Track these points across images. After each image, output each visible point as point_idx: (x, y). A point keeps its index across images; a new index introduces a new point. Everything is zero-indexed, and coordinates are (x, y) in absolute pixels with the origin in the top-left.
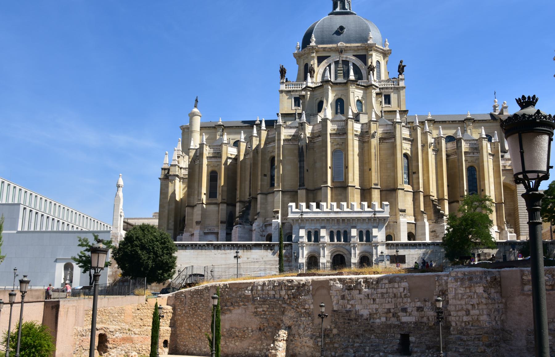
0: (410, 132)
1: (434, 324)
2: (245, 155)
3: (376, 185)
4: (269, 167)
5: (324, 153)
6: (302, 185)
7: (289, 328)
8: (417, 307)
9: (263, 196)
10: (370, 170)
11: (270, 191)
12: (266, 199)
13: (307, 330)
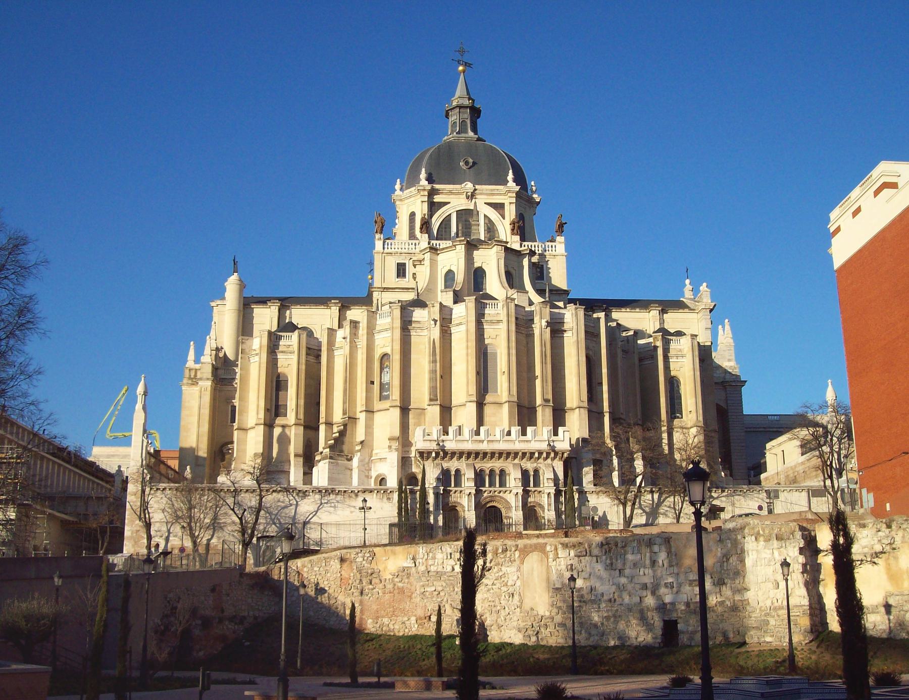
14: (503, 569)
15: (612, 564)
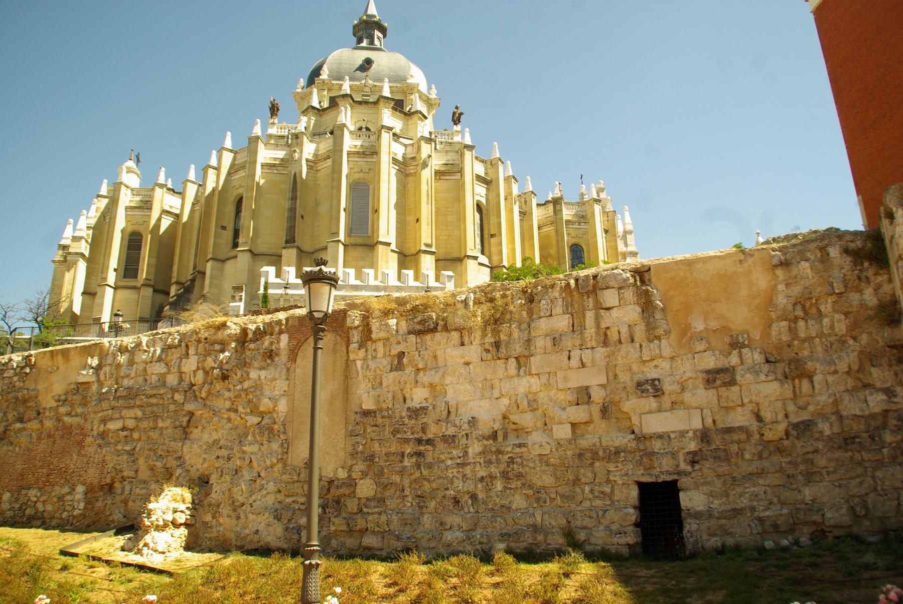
0: (486, 169)
1: (787, 434)
2: (193, 204)
3: (429, 246)
4: (233, 214)
5: (335, 183)
6: (290, 241)
7: (201, 484)
8: (708, 372)
9: (216, 264)
10: (418, 220)
11: (233, 253)
12: (222, 270)
13: (262, 487)
14: (253, 375)
15: (497, 345)
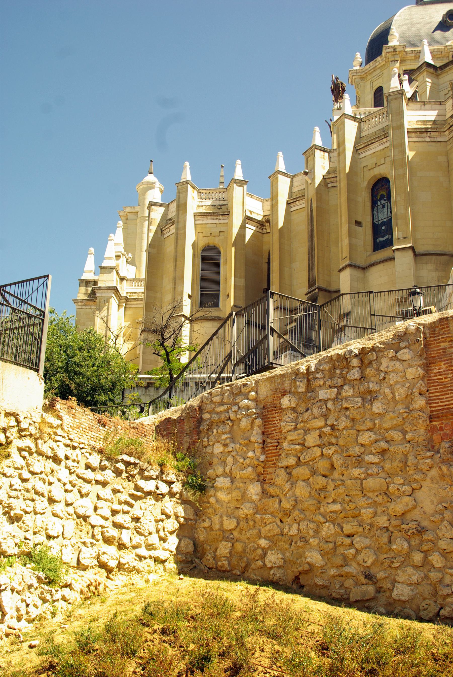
2: (288, 204)
